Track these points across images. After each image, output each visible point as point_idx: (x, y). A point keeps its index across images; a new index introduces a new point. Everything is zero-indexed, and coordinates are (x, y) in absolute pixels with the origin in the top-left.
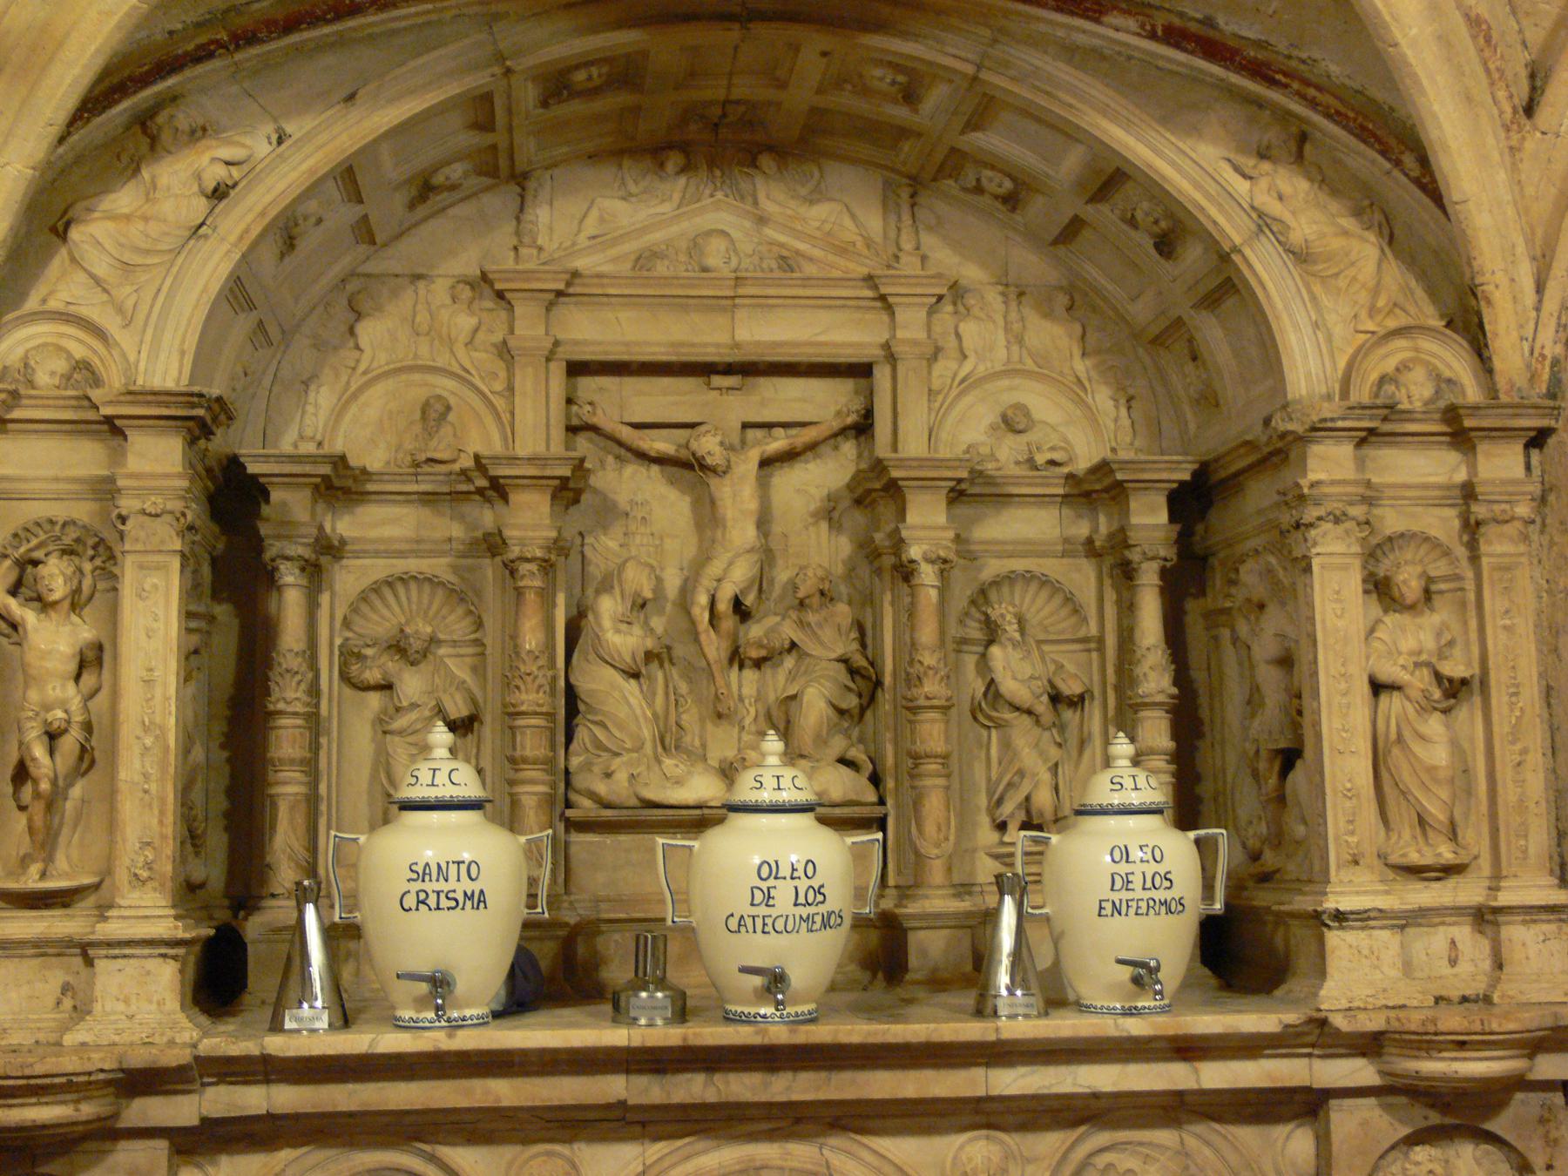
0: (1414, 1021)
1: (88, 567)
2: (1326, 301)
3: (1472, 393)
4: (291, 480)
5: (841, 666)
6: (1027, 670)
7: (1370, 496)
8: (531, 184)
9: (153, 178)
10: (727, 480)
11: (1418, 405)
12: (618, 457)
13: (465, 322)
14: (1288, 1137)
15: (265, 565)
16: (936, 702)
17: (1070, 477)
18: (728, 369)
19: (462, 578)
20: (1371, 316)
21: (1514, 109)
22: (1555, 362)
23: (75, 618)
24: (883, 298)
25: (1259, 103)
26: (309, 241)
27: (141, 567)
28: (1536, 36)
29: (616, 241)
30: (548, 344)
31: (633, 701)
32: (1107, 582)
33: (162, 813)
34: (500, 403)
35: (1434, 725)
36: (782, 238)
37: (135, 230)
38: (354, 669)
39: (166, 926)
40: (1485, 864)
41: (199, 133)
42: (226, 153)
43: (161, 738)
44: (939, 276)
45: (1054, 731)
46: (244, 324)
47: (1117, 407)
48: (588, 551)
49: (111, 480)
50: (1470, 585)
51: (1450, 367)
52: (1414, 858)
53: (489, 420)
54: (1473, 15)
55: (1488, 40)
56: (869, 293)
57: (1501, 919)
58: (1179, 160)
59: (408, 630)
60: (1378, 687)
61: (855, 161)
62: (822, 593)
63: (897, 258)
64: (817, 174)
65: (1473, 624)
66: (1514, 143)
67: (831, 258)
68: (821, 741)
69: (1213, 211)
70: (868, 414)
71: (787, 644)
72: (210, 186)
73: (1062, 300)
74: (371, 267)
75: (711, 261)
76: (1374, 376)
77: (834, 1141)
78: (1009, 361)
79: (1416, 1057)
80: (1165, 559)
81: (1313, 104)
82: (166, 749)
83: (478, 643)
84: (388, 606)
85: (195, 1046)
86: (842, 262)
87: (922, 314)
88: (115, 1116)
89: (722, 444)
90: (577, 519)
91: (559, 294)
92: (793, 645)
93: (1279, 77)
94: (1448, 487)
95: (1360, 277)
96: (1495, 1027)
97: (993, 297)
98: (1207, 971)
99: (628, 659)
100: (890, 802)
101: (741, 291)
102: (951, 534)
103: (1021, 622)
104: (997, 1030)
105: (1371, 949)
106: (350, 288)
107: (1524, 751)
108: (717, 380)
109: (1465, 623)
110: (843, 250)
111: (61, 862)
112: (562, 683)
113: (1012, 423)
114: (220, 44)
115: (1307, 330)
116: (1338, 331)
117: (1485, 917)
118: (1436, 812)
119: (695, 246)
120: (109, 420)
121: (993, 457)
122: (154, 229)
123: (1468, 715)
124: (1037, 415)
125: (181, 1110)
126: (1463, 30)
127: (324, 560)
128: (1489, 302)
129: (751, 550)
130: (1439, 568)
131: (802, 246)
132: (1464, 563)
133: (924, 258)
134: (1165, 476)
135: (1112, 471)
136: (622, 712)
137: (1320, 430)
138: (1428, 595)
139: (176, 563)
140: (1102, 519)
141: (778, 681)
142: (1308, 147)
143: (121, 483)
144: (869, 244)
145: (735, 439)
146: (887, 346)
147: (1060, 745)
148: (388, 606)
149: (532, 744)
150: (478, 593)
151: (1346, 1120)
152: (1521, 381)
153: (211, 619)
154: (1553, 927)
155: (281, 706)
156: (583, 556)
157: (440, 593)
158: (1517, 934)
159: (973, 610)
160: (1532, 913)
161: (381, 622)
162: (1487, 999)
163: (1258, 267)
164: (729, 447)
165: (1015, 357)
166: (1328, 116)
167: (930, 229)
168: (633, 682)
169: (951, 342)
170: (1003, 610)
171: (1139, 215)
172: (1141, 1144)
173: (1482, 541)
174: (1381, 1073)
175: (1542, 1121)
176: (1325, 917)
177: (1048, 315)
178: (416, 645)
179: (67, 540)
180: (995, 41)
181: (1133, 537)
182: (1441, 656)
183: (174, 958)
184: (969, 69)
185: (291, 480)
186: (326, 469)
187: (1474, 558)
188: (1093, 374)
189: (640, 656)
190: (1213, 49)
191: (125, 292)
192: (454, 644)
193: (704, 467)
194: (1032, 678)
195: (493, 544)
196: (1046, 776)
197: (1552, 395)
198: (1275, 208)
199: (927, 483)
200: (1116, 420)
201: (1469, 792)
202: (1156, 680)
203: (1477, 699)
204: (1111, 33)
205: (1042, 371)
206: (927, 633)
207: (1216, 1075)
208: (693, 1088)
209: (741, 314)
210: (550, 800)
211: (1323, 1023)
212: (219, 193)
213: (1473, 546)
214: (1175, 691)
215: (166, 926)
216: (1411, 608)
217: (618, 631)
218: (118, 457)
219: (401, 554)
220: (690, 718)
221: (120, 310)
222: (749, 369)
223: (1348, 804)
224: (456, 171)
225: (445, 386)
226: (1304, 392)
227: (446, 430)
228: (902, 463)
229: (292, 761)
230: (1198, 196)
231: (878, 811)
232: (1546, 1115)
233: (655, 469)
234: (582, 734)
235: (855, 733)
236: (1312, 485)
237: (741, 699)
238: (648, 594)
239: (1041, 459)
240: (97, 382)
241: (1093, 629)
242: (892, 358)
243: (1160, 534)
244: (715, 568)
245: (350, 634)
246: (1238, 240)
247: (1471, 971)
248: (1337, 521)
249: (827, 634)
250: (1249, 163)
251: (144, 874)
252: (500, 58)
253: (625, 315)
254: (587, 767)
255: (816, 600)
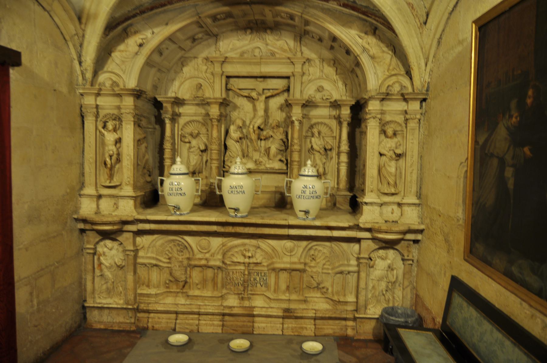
0: (376, 226)
1: (117, 123)
2: (378, 68)
3: (410, 90)
4: (167, 102)
5: (281, 141)
6: (319, 143)
7: (383, 113)
8: (218, 37)
9: (127, 42)
10: (258, 102)
11: (396, 92)
12: (238, 96)
13: (205, 68)
14: (354, 246)
15: (161, 119)
16: (297, 150)
17: (331, 102)
18: (261, 77)
19: (204, 121)
20: (388, 71)
21: (421, 24)
22: (429, 83)
23: (115, 133)
24: (292, 62)
25: (366, 21)
26: (166, 53)
27: (126, 124)
28: (428, 6)
29: (236, 50)
30: (221, 72)
31: (237, 147)
32: (338, 125)
33: (131, 172)
34: (212, 84)
35: (393, 163)
36: (271, 48)
37: (124, 54)
38: (183, 139)
39: (131, 193)
40: (402, 193)
41: (136, 32)
42: (142, 37)
43: (130, 157)
44: (304, 57)
45: (325, 156)
46: (153, 71)
47: (343, 87)
48: (231, 116)
49: (119, 106)
50: (405, 133)
51: (405, 83)
52: (386, 191)
53: (210, 89)
54: (408, 3)
55: (413, 8)
56: (289, 61)
57: (402, 205)
58: (347, 35)
59: (193, 132)
60: (381, 155)
61: (288, 31)
62: (277, 126)
63: (296, 53)
64: (279, 33)
65: (405, 141)
66: (421, 32)
67: (282, 53)
68: (275, 156)
69: (354, 47)
70: (289, 87)
71: (270, 136)
72: (138, 44)
73: (332, 62)
74: (186, 55)
75: (256, 54)
76: (387, 86)
77: (260, 240)
78: (320, 76)
79: (378, 234)
80: (348, 121)
81: (377, 21)
82: (131, 159)
83: (208, 134)
84: (190, 126)
85: (134, 216)
86: (284, 54)
87: (301, 66)
88: (122, 228)
89: (257, 94)
90: (228, 109)
91: (223, 62)
92: (272, 136)
93: (370, 15)
94: (402, 111)
95: (386, 62)
96: (393, 229)
97: (317, 62)
98: (350, 208)
99: (236, 139)
100: (289, 169)
101: (262, 61)
102: (301, 115)
103: (319, 133)
104: (288, 222)
105: (373, 210)
106: (183, 59)
107: (413, 170)
108: (259, 79)
109: (403, 141)
110: (285, 51)
111: (115, 180)
112: (223, 143)
113: (320, 89)
114: (137, 14)
115: (373, 74)
116: (380, 74)
117: (399, 205)
118: (392, 182)
119: (253, 51)
120: (119, 94)
121: (315, 97)
122: (128, 53)
123: (401, 162)
124: (325, 88)
125: (134, 228)
126: (406, 6)
127: (175, 117)
128: (412, 69)
129: (262, 116)
130: (398, 128)
131: (276, 50)
132: (404, 128)
133: (302, 53)
134: (349, 103)
135: (337, 102)
136: (234, 149)
137: (371, 98)
138: (395, 134)
139: (132, 123)
140: (338, 111)
141: (269, 143)
142: (377, 32)
143: (121, 107)
144: (290, 49)
145: (261, 92)
146: (292, 73)
147: (326, 159)
148: (190, 126)
149: (215, 156)
150: (207, 124)
151: (363, 243)
152: (420, 88)
153: (155, 128)
154: (414, 208)
155: (166, 147)
156: (230, 116)
157: (200, 124)
158: (406, 208)
159: (310, 130)
160: (409, 205)
161: (189, 129)
162: (397, 222)
163: (363, 60)
164: (259, 94)
165: (321, 75)
166: (381, 24)
167: (304, 46)
168: (238, 143)
169: (307, 72)
170: (315, 131)
171: (341, 46)
172: (323, 245)
173: (408, 124)
174: (372, 236)
175: (407, 247)
176: (363, 203)
177: (329, 65)
178: (194, 135)
179: (113, 118)
180: (305, 8)
181: (341, 116)
182: (396, 148)
183: (133, 199)
184: (300, 14)
185: (167, 102)
186: (173, 100)
187: (406, 127)
188: (338, 79)
189: (238, 138)
190: (354, 8)
191: (123, 67)
192: (203, 134)
193: (253, 99)
194: (321, 145)
195: (207, 115)
196: (321, 165)
197: (427, 90)
198: (367, 46)
199: (297, 104)
200: (342, 90)
201: (401, 177)
202: (345, 147)
203: (404, 158)
204: (332, 5)
205: (327, 78)
206: (296, 135)
207: (336, 234)
208: (230, 229)
209: (262, 65)
210: (218, 168)
211: (358, 225)
212: (141, 45)
213: (406, 124)
214: (349, 149)
215: (131, 193)
216: (391, 138)
217: (234, 133)
218: (121, 101)
219: (192, 116)
220: (251, 149)
221: (122, 70)
222: (265, 77)
223: (371, 180)
224: (200, 35)
225: (201, 81)
226: (371, 88)
227: (201, 91)
228: (291, 100)
229: (168, 158)
230: (351, 43)
231: (286, 171)
232: (408, 246)
233: (245, 98)
234: (227, 153)
235: (284, 154)
236: (369, 110)
237: (261, 146)
238: (241, 125)
239: (324, 98)
240: (118, 85)
241: (335, 135)
242: (294, 76)
243: (347, 116)
244: (254, 120)
245: (182, 132)
246: (359, 53)
247: (396, 216)
248: (374, 118)
249: (278, 134)
250: (363, 35)
251: (128, 183)
252: (198, 14)
253: (238, 66)
254: (228, 160)
255: (275, 127)
